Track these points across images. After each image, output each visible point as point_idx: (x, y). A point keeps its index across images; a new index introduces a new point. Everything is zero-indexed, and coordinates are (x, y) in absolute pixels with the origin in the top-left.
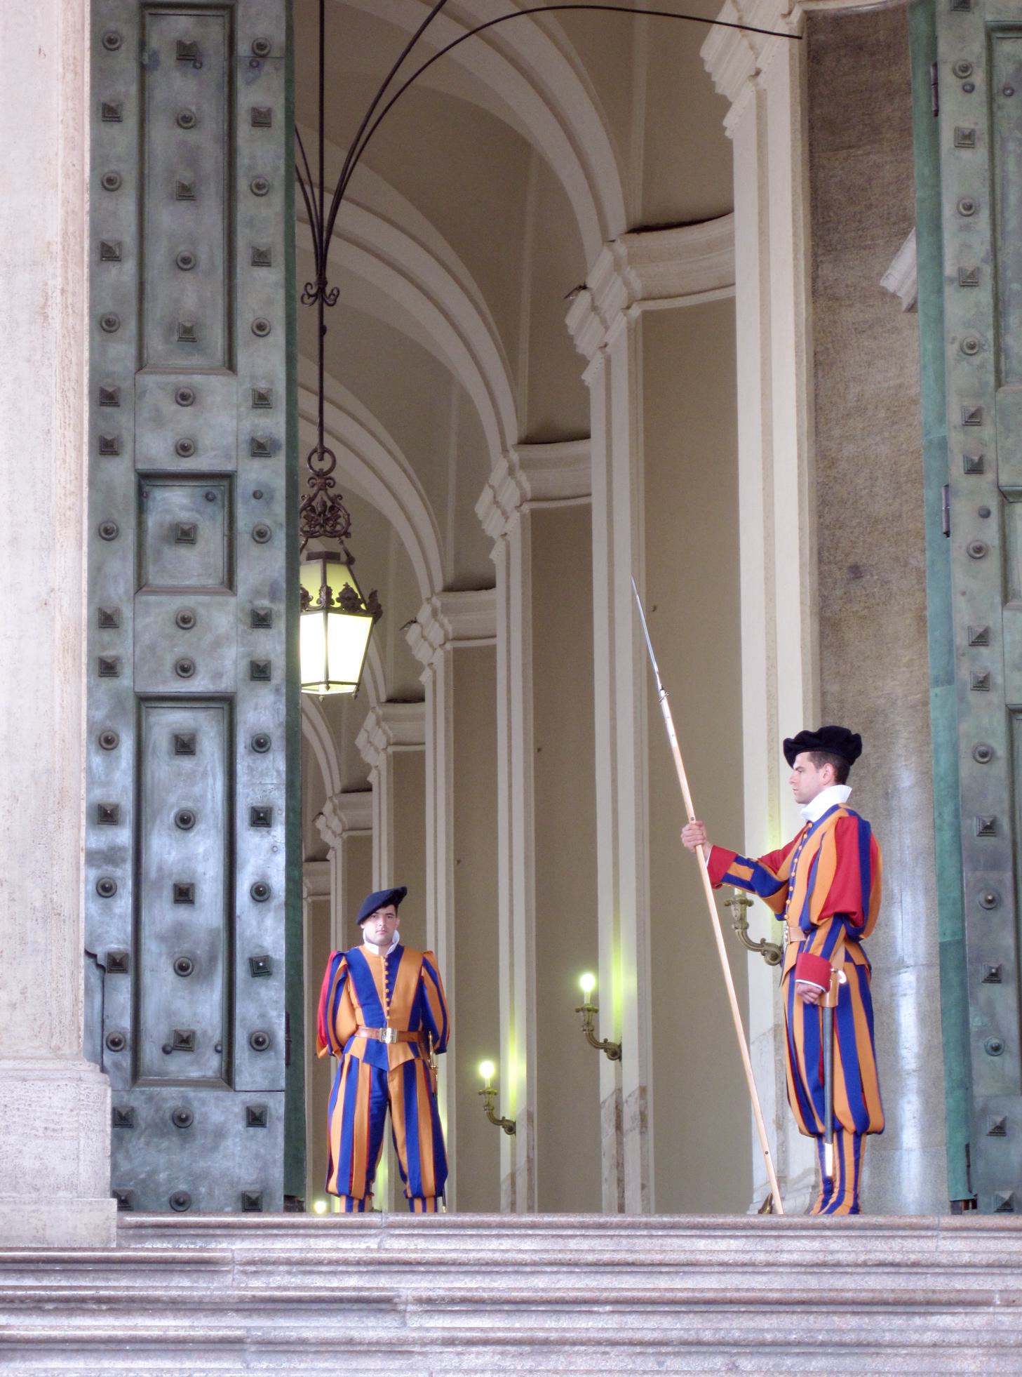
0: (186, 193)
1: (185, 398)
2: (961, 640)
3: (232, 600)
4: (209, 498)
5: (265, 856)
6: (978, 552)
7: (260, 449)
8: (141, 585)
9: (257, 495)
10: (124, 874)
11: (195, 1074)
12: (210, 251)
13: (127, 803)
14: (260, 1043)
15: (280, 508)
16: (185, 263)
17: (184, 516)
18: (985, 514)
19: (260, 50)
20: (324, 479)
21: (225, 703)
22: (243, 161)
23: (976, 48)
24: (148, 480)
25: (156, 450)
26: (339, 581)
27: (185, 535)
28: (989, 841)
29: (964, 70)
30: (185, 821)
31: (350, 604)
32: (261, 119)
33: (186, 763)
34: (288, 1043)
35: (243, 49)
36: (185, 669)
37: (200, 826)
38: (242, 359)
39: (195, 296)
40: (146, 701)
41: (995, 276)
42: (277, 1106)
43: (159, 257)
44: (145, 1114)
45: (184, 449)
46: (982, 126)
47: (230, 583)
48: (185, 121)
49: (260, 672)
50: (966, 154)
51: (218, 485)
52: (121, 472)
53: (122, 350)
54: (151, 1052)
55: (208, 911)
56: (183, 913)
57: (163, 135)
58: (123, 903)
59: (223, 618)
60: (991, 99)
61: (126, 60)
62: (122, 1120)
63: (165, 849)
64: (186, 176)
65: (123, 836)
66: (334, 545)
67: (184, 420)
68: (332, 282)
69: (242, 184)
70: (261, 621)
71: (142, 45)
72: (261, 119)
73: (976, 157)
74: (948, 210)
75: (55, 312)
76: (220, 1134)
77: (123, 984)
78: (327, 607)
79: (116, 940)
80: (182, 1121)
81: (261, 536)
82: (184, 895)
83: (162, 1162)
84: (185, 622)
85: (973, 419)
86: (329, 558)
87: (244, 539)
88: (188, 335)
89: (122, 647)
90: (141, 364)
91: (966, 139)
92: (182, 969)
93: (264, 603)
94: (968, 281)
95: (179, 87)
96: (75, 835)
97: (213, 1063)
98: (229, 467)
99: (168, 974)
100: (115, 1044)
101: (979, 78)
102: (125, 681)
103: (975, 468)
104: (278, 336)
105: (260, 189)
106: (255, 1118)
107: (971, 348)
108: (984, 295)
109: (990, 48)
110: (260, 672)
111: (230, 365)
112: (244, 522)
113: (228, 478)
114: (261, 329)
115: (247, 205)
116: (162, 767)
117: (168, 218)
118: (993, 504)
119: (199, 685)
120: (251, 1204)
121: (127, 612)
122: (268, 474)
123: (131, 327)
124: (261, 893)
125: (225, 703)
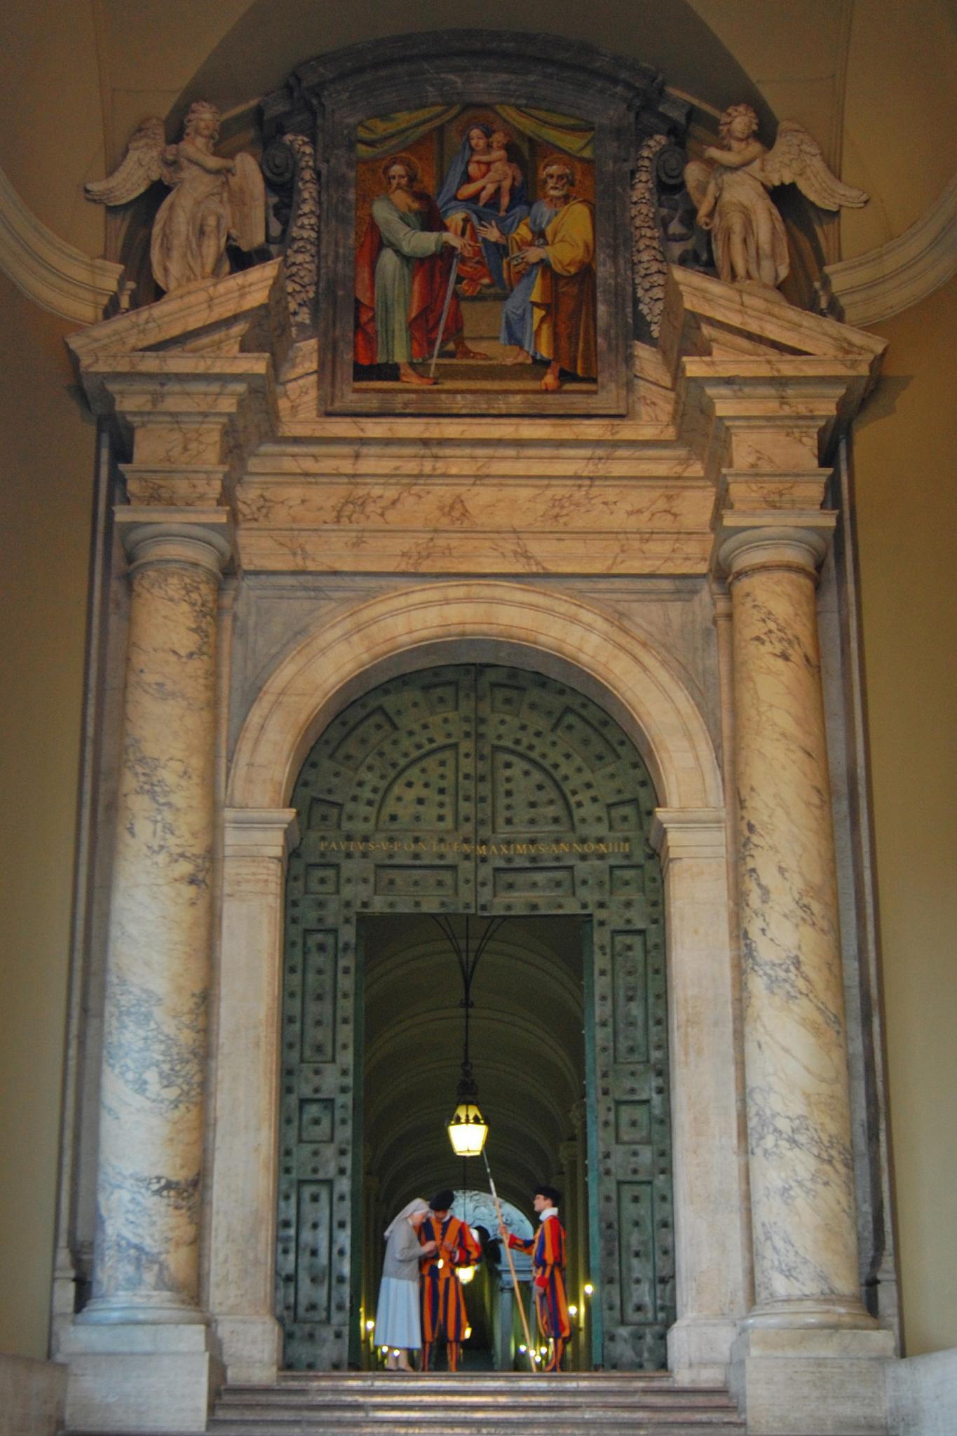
0: (319, 998)
1: (317, 1072)
2: (601, 1156)
3: (333, 1145)
4: (326, 1108)
5: (344, 1238)
6: (606, 1124)
7: (344, 1090)
8: (300, 1141)
9: (342, 1107)
10: (292, 1245)
11: (317, 1319)
12: (328, 1018)
13: (293, 1219)
14: (340, 1307)
15: (350, 1111)
16: (319, 1023)
17: (316, 1115)
18: (609, 1109)
19: (346, 947)
20: (467, 1074)
21: (329, 1183)
22: (340, 985)
23: (606, 939)
24: (303, 1102)
25: (306, 1091)
26: (473, 1111)
27: (316, 1122)
28: (609, 1232)
29: (602, 948)
30: (315, 1226)
31: (477, 1120)
32: (346, 971)
33: (315, 1205)
34: (351, 1308)
35: (341, 945)
36: (315, 1171)
37: (320, 1229)
38: (338, 1057)
39: (322, 1035)
40: (301, 1183)
41: (615, 1022)
42: (346, 1330)
43: (309, 1020)
44: (298, 1334)
45: (316, 1090)
46: (609, 967)
47: (332, 1140)
48: (320, 972)
49: (342, 1171)
50: (603, 978)
51: (328, 1103)
52: (293, 1100)
53: (295, 1055)
54: (301, 1310)
55: (323, 1259)
56: (314, 1259)
57: (311, 977)
58: (292, 1257)
59: (329, 1151)
60: (613, 957)
61: (298, 951)
62: (288, 1337)
63: (307, 1235)
64: (320, 991)
65: (292, 1232)
66: (469, 1098)
67: (316, 1080)
68: (472, 998)
69: (339, 994)
70: (343, 1152)
71: (305, 944)
72: (346, 971)
73: (607, 979)
74: (597, 998)
75: (262, 1044)
76: (325, 1341)
77: (292, 1285)
78: (467, 1121)
79: (289, 1267)
80: (311, 1336)
81: (344, 1122)
82: (314, 1253)
83: (302, 1351)
84: (316, 1153)
85: (605, 1075)
86: (468, 1103)
87: (337, 1123)
88: (319, 1048)
89: (293, 1162)
90: (302, 1061)
91: (603, 973)
92: (313, 1280)
93: (344, 1146)
94: (604, 1024)
95: (317, 959)
96: (266, 1234)
97: (324, 1315)
98: (332, 1096)
99: (308, 1281)
100: (288, 1308)
101: (608, 950)
102: (294, 1175)
103: (606, 1092)
104: (351, 1049)
105: (345, 996)
106: (338, 1335)
107: (604, 1049)
108: (609, 1029)
109: (612, 938)
110: (342, 1171)
111: (333, 1060)
112: (338, 1115)
113: (332, 1101)
114: (345, 1047)
115: (341, 1002)
116: (307, 1206)
117: (312, 1007)
118: (612, 1106)
119: (321, 1176)
120: (336, 1367)
121: (295, 1149)
122: (348, 1099)
123: (298, 1047)
124: (341, 1252)
125: (329, 1183)
